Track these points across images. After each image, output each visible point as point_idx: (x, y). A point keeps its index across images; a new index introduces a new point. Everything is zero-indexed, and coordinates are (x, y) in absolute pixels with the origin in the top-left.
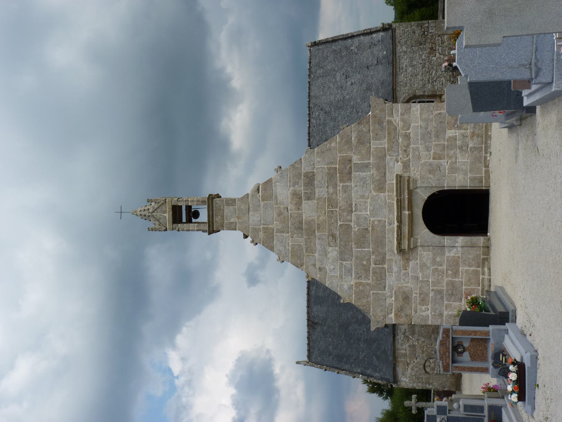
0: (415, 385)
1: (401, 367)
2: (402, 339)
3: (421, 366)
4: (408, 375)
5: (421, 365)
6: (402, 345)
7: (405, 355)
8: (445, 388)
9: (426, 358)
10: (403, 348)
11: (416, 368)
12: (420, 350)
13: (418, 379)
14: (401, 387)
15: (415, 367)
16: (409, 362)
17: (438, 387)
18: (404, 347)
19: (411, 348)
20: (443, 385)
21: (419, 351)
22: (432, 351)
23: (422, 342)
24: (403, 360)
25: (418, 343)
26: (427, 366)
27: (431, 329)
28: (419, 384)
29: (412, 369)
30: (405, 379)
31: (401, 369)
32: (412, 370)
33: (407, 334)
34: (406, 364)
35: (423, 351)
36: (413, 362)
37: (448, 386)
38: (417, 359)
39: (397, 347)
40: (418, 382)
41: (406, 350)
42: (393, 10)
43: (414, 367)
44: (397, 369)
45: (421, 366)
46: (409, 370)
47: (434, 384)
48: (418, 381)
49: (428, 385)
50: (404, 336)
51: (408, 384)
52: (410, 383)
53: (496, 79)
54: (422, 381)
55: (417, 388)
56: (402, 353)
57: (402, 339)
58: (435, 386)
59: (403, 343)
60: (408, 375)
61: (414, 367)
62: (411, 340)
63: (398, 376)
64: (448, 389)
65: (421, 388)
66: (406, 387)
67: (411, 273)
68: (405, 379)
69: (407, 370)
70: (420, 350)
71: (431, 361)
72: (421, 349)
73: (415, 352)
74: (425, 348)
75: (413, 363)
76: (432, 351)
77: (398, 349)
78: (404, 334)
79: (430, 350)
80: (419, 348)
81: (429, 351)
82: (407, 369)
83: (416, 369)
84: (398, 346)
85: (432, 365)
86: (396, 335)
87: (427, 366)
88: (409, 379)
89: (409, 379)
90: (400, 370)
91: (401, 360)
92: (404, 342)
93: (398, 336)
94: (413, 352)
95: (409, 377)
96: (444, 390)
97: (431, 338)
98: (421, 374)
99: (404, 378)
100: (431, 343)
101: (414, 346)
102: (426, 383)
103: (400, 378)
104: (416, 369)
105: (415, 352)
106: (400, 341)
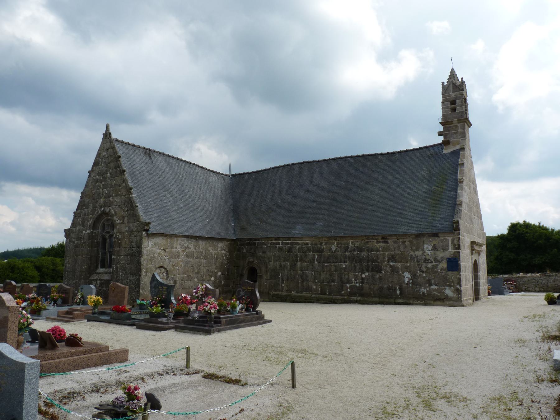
0: (145, 257)
1: (163, 242)
2: (184, 244)
3: (162, 264)
4: (154, 249)
5: (163, 264)
6: (180, 244)
7: (172, 248)
8: (142, 289)
9: (168, 268)
10: (178, 246)
11: (161, 258)
12: (175, 263)
13: (150, 260)
14: (143, 241)
15: (162, 257)
16: (167, 250)
17: (143, 282)
18: (179, 246)
19: (177, 253)
20: (145, 287)
21: (174, 261)
22: (174, 275)
23: (181, 264)
24: (169, 244)
25: (181, 261)
26: (161, 270)
27: (191, 274)
28: (146, 261)
29: (159, 254)
30: (150, 245)
31: (161, 242)
32: (158, 254)
33: (187, 251)
34: (164, 248)
35: (174, 266)
36: (166, 255)
37: (144, 293)
38: (168, 259)
39: (179, 239)
40: (148, 260)
41: (176, 248)
42: (523, 221)
43: (162, 256)
44: (161, 238)
45: (162, 264)
46: (158, 251)
47: (146, 278)
48: (149, 260)
49: (145, 270)
50: (186, 247)
51: (146, 249)
52: (147, 251)
53: (249, 327)
54: (148, 264)
55: (142, 259)
56: (174, 244)
57: (184, 244)
58: (144, 279)
59: (181, 246)
60: (154, 249)
61: (162, 256)
62: (182, 254)
63: (154, 238)
64: (141, 293)
65: (142, 263)
66: (143, 246)
67: (291, 242)
68: (150, 245)
69: (159, 248)
70: (175, 263)
71: (165, 274)
72: (176, 263)
73: (173, 257)
74: (176, 268)
75: (165, 256)
76: (174, 275)
77: (177, 240)
78: (188, 247)
79: (174, 272)
80: (176, 262)
81: (174, 272)
82: (160, 249)
83: (159, 257)
84: (180, 240)
85: (161, 275)
86: (188, 239)
87: (161, 270)
88: (150, 250)
89: (150, 250)
90: (159, 240)
91: (169, 242)
92: (182, 247)
93: (186, 241)
94: (174, 256)
95: (152, 250)
96: (141, 289)
97: (184, 274)
98: (155, 264)
99: (152, 244)
100: (180, 274)
101: (178, 256)
102: (147, 269)
103: (152, 240)
104: (159, 257)
105: (173, 257)
106: (183, 242)
